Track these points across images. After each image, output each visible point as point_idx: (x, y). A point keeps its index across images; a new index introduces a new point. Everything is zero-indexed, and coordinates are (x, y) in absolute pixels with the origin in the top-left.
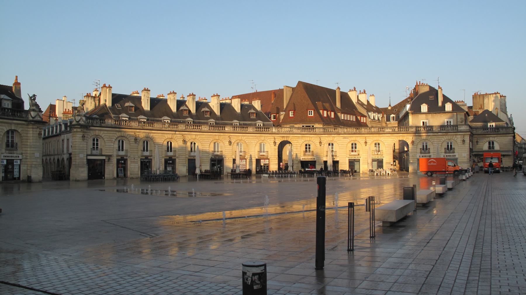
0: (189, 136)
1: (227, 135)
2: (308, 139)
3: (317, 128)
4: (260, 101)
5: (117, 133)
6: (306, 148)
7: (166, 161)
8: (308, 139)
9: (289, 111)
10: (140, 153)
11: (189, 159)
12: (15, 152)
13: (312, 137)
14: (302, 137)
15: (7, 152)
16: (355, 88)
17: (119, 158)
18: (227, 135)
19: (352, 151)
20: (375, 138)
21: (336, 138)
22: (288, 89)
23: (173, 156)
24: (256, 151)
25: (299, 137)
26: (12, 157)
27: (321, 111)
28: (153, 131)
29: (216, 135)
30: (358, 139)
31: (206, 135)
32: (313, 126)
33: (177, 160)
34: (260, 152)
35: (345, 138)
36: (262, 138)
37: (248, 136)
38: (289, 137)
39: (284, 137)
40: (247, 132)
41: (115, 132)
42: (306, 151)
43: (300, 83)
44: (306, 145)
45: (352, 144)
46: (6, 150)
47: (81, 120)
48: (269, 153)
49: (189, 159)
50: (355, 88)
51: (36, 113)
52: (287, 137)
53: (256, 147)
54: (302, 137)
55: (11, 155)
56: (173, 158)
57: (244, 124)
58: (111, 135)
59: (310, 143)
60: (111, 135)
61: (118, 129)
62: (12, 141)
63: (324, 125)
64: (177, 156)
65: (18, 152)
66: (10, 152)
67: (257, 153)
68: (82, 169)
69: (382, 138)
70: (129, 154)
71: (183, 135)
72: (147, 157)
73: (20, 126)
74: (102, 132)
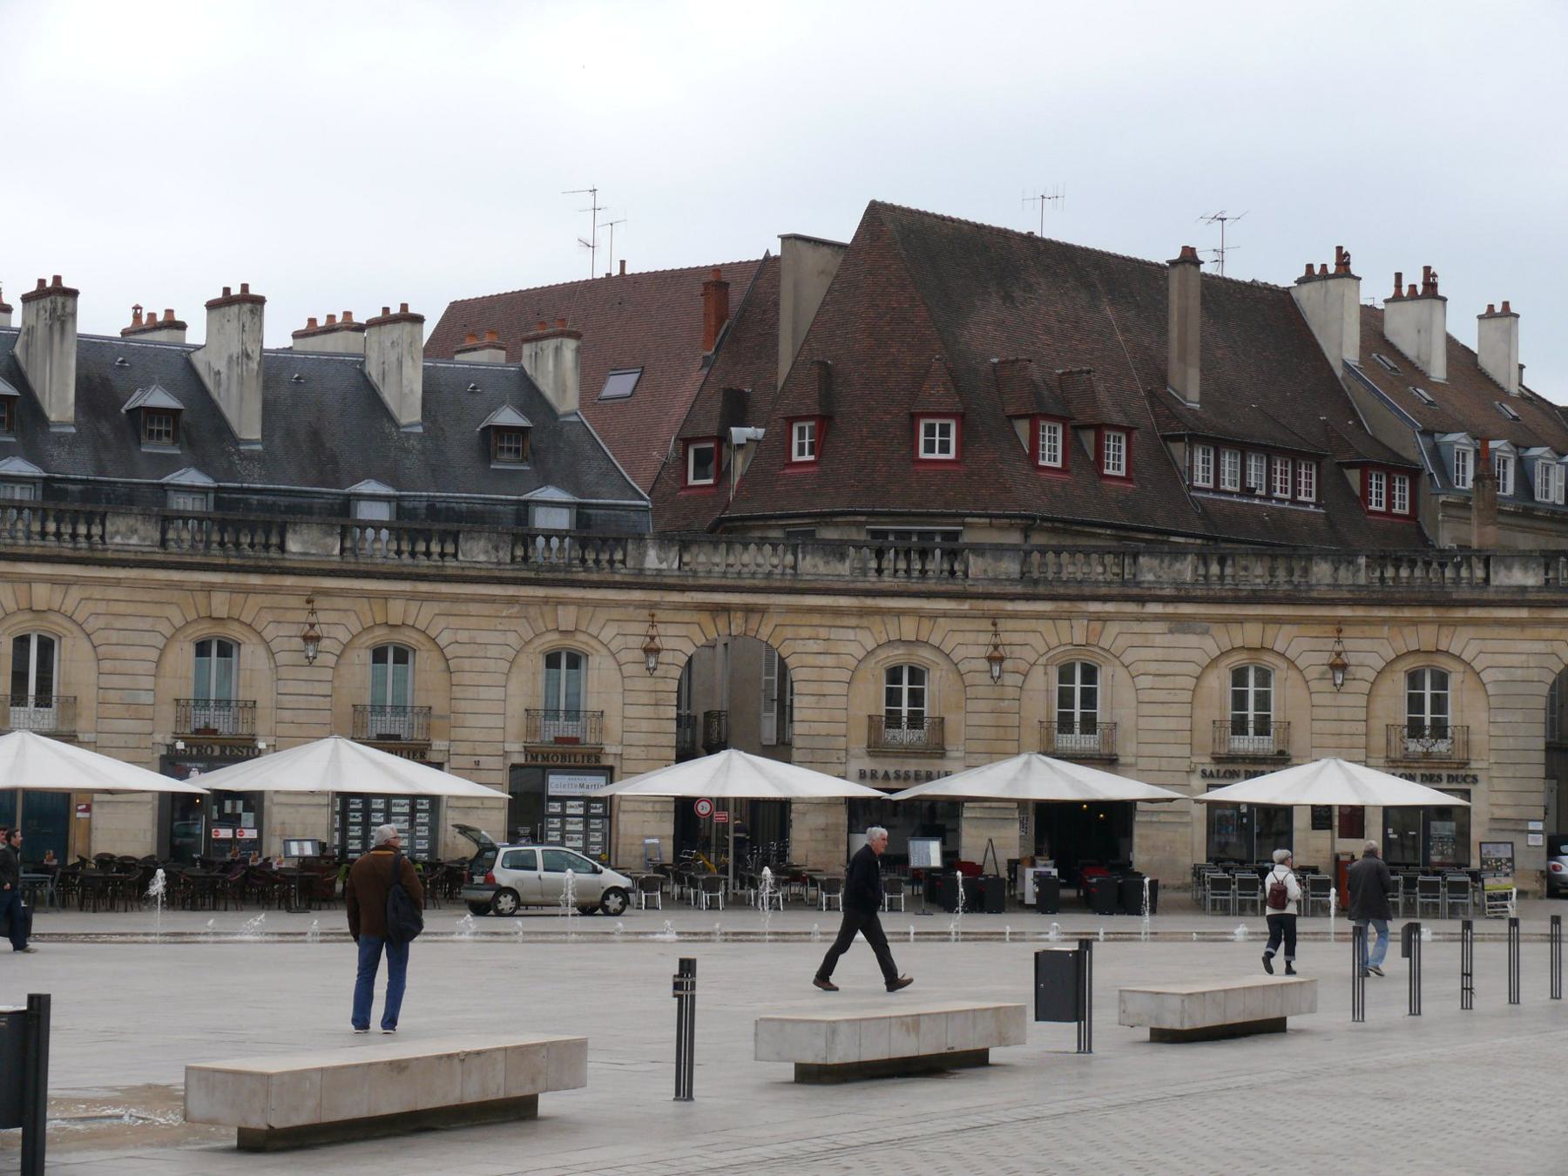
1: (291, 592)
2: (908, 628)
3: (979, 550)
4: (569, 346)
6: (893, 697)
8: (908, 628)
9: (790, 421)
13: (934, 616)
14: (863, 612)
16: (1343, 259)
18: (291, 592)
19: (1239, 727)
20: (1412, 639)
21: (1113, 628)
22: (811, 257)
24: (517, 706)
25: (838, 612)
27: (1022, 428)
29: (209, 588)
30: (1282, 638)
31: (132, 585)
32: (955, 536)
34: (552, 713)
35: (1180, 625)
36: (567, 617)
37: (455, 599)
38: (763, 610)
39: (726, 609)
42: (893, 720)
43: (877, 214)
44: (894, 675)
45: (1239, 676)
48: (613, 723)
50: (1343, 259)
52: (749, 610)
53: (513, 687)
54: (863, 612)
57: (433, 511)
59: (923, 656)
63: (1026, 532)
67: (516, 724)
69: (1465, 633)
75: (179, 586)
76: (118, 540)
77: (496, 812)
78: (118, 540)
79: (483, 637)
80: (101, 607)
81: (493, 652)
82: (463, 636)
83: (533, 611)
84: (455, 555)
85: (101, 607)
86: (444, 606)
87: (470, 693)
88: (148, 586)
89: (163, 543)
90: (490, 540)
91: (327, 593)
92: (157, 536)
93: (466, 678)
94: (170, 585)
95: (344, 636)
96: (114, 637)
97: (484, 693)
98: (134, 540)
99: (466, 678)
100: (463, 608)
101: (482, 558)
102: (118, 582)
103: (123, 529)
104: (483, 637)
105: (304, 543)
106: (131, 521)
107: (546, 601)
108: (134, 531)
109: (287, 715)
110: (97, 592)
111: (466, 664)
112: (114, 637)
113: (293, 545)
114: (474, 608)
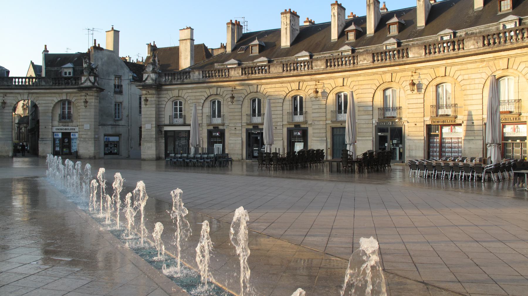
0: (331, 82)
1: (407, 70)
5: (207, 90)
7: (290, 132)
10: (245, 120)
11: (333, 129)
12: (70, 124)
15: (61, 124)
17: (211, 128)
23: (219, 125)
26: (66, 129)
28: (263, 81)
31: (364, 75)
33: (310, 131)
40: (461, 52)
41: (203, 90)
46: (59, 122)
47: (149, 79)
49: (333, 129)
51: (86, 78)
55: (65, 128)
56: (303, 126)
58: (198, 94)
60: (198, 94)
61: (205, 85)
62: (69, 113)
64: (309, 122)
65: (74, 124)
66: (64, 124)
68: (149, 145)
70: (227, 122)
71: (318, 81)
72: (256, 126)
73: (73, 95)
74: (185, 91)
75: (376, 73)
76: (361, 63)
77: (479, 141)
78: (361, 63)
79: (473, 76)
80: (357, 83)
81: (477, 81)
82: (466, 77)
83: (491, 63)
84: (463, 48)
85: (357, 83)
86: (459, 67)
87: (470, 97)
88: (368, 75)
89: (374, 61)
90: (474, 39)
91: (420, 68)
92: (371, 60)
93: (468, 92)
94: (374, 74)
95: (427, 83)
96: (360, 91)
97: (474, 97)
98: (365, 62)
99: (468, 92)
100: (465, 67)
101: (472, 47)
102: (360, 75)
103: (362, 59)
104: (473, 76)
105: (414, 53)
106: (364, 57)
107: (495, 59)
108: (365, 59)
109: (410, 111)
110: (355, 79)
111: (468, 87)
112: (360, 91)
113: (410, 55)
114: (469, 66)
